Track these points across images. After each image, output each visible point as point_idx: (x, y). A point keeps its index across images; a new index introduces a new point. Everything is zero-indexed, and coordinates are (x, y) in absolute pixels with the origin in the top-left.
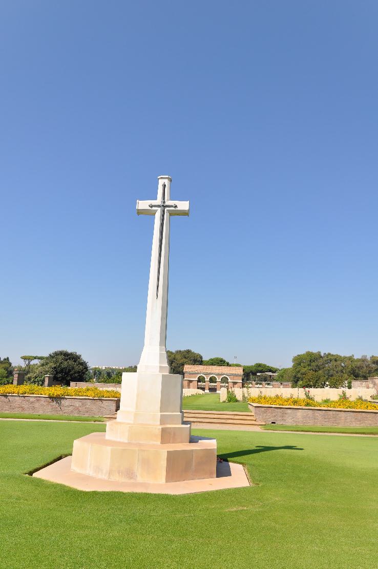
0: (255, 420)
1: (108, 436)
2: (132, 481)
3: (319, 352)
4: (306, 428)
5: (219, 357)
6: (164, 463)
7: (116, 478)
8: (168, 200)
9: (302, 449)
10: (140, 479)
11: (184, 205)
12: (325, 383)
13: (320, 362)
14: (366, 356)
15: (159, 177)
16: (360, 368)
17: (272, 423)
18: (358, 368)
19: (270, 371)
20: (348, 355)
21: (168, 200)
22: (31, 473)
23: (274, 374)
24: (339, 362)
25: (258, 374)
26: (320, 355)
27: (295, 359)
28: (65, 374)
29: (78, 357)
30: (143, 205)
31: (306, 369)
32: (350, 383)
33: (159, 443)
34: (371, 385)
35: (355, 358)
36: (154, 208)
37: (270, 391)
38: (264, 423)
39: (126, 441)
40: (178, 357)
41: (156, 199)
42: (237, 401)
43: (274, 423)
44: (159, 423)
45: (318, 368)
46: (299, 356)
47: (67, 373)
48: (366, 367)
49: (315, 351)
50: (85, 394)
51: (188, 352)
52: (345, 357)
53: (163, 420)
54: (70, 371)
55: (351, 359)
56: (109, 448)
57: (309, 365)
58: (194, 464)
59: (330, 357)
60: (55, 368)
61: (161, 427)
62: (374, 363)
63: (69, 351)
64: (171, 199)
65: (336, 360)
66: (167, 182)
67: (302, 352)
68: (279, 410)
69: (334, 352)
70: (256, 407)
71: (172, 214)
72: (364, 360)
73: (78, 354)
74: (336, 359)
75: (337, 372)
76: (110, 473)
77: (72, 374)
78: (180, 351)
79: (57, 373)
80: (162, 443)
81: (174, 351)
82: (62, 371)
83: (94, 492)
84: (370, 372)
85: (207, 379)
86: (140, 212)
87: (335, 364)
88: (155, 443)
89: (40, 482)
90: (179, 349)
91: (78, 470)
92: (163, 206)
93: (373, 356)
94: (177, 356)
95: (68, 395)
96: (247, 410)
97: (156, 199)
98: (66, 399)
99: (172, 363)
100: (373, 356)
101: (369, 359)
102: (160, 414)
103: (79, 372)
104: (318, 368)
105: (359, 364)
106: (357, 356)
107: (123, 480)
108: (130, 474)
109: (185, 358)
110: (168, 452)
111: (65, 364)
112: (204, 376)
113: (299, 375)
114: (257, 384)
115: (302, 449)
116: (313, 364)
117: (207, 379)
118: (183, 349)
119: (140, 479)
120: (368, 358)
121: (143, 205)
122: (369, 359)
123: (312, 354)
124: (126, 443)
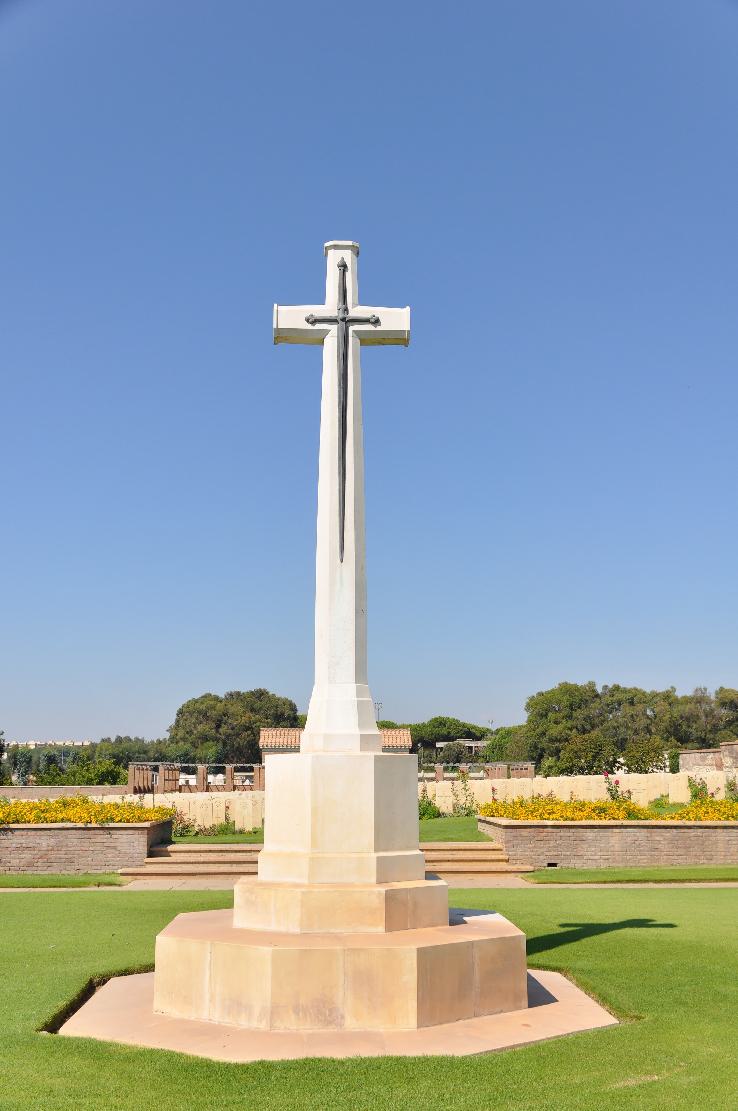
0: (507, 861)
1: (241, 917)
2: (332, 1030)
3: (592, 685)
4: (635, 874)
6: (410, 978)
7: (290, 1024)
8: (354, 305)
9: (671, 926)
10: (351, 1024)
11: (396, 319)
12: (615, 761)
13: (594, 709)
14: (705, 689)
15: (327, 244)
16: (690, 719)
17: (550, 865)
18: (688, 719)
20: (661, 688)
21: (354, 305)
22: (54, 1026)
23: (479, 744)
24: (639, 707)
25: (439, 745)
26: (594, 691)
27: (528, 707)
30: (290, 317)
31: (560, 727)
32: (675, 758)
33: (381, 929)
34: (728, 761)
35: (679, 694)
36: (318, 326)
37: (483, 788)
38: (531, 868)
39: (297, 930)
40: (236, 708)
41: (321, 301)
42: (439, 815)
43: (555, 865)
44: (374, 880)
45: (592, 723)
46: (541, 694)
48: (707, 716)
49: (580, 680)
50: (60, 816)
51: (260, 694)
52: (655, 695)
53: (385, 871)
55: (668, 697)
56: (266, 951)
57: (569, 717)
58: (477, 977)
59: (618, 696)
61: (382, 889)
62: (723, 704)
64: (363, 301)
65: (632, 703)
66: (348, 256)
67: (549, 684)
68: (563, 833)
69: (627, 682)
70: (506, 827)
71: (365, 340)
72: (699, 699)
74: (633, 698)
75: (636, 732)
76: (274, 1012)
78: (238, 693)
80: (389, 928)
81: (222, 695)
83: (261, 1063)
84: (715, 729)
86: (283, 336)
87: (629, 710)
88: (372, 930)
89: (96, 1051)
91: (175, 1012)
92: (343, 320)
93: (722, 689)
94: (232, 709)
95: (18, 822)
96: (480, 837)
97: (321, 301)
98: (12, 830)
99: (218, 726)
100: (722, 689)
101: (713, 697)
102: (374, 855)
104: (592, 723)
105: (687, 709)
106: (684, 691)
107: (307, 1028)
108: (325, 1011)
109: (253, 710)
110: (421, 952)
113: (544, 743)
114: (446, 769)
115: (671, 926)
116: (578, 714)
118: (244, 689)
119: (351, 1024)
120: (712, 694)
121: (290, 317)
122: (713, 697)
123: (576, 688)
124: (294, 935)
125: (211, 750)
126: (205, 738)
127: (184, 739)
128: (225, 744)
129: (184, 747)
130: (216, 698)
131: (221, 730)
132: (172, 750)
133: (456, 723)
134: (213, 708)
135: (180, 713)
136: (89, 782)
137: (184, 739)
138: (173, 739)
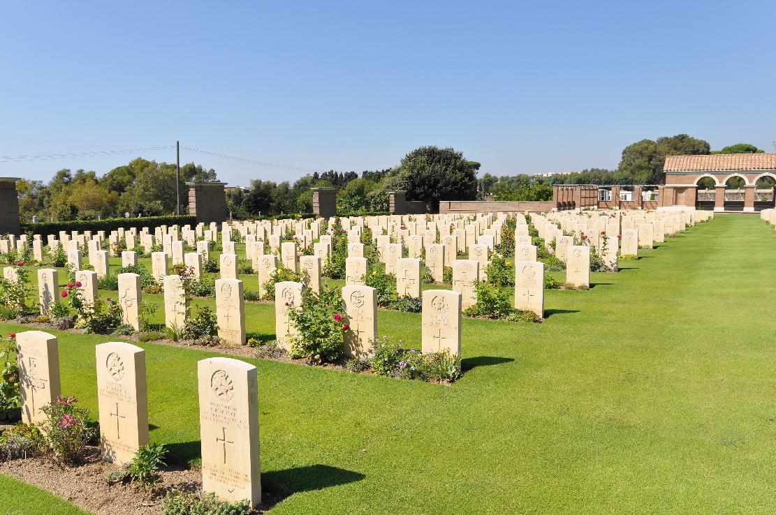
5: (744, 143)
28: (429, 188)
29: (457, 157)
40: (661, 148)
47: (433, 186)
54: (437, 181)
60: (410, 177)
63: (441, 146)
73: (455, 151)
77: (441, 188)
78: (667, 138)
79: (414, 185)
82: (423, 182)
85: (720, 183)
90: (663, 136)
103: (455, 183)
111: (428, 169)
112: (713, 177)
117: (720, 183)
118: (671, 134)
125: (645, 175)
126: (640, 168)
127: (625, 169)
129: (627, 173)
130: (650, 142)
131: (651, 162)
132: (615, 177)
134: (647, 148)
135: (624, 152)
136: (529, 199)
137: (625, 169)
138: (621, 169)
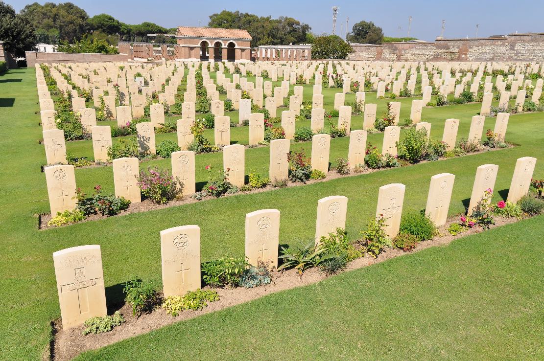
3: (238, 12)
19: (160, 31)
20: (265, 17)
26: (238, 15)
49: (233, 11)
52: (263, 19)
55: (268, 19)
59: (248, 18)
72: (280, 22)
100: (287, 18)
106: (275, 18)
128: (61, 29)
133: (154, 26)
